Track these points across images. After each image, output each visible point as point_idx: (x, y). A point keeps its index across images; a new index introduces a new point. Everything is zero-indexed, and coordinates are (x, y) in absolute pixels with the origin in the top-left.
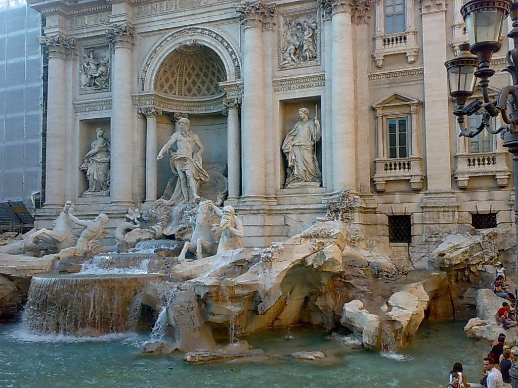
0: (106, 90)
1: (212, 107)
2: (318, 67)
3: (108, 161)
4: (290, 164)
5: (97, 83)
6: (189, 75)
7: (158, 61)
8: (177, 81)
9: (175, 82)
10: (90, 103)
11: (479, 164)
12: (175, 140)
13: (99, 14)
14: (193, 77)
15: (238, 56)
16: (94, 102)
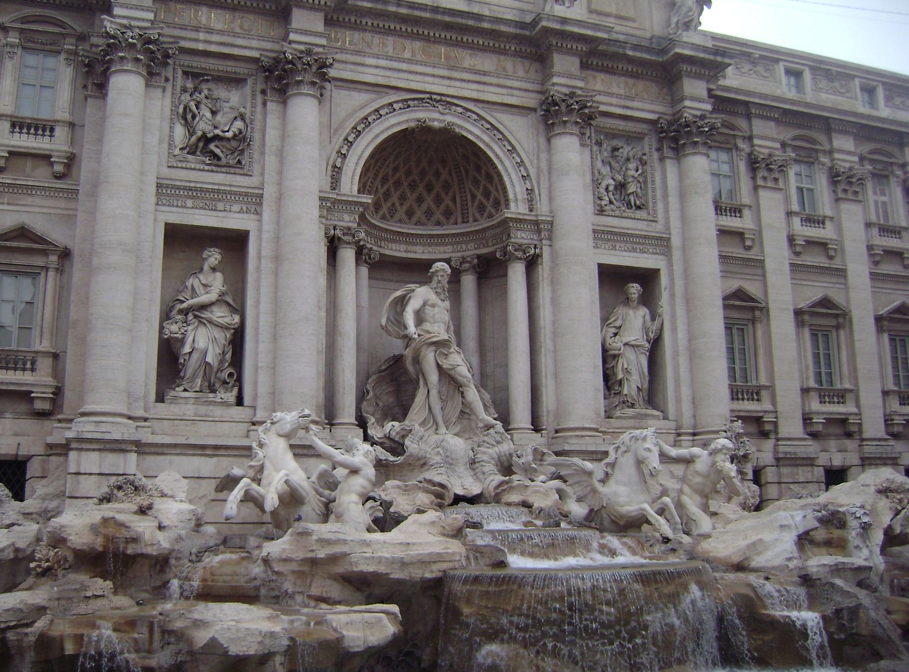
0: (237, 170)
1: (419, 249)
2: (654, 224)
3: (236, 326)
4: (620, 376)
5: (217, 151)
6: (385, 180)
7: (372, 141)
8: (369, 183)
9: (365, 184)
10: (202, 190)
11: (829, 402)
12: (422, 302)
13: (237, 14)
14: (391, 182)
15: (530, 172)
16: (213, 191)
